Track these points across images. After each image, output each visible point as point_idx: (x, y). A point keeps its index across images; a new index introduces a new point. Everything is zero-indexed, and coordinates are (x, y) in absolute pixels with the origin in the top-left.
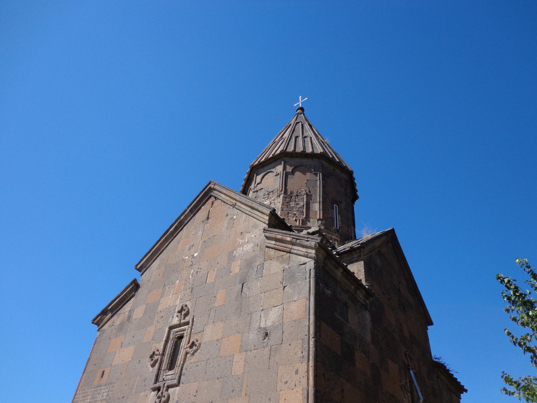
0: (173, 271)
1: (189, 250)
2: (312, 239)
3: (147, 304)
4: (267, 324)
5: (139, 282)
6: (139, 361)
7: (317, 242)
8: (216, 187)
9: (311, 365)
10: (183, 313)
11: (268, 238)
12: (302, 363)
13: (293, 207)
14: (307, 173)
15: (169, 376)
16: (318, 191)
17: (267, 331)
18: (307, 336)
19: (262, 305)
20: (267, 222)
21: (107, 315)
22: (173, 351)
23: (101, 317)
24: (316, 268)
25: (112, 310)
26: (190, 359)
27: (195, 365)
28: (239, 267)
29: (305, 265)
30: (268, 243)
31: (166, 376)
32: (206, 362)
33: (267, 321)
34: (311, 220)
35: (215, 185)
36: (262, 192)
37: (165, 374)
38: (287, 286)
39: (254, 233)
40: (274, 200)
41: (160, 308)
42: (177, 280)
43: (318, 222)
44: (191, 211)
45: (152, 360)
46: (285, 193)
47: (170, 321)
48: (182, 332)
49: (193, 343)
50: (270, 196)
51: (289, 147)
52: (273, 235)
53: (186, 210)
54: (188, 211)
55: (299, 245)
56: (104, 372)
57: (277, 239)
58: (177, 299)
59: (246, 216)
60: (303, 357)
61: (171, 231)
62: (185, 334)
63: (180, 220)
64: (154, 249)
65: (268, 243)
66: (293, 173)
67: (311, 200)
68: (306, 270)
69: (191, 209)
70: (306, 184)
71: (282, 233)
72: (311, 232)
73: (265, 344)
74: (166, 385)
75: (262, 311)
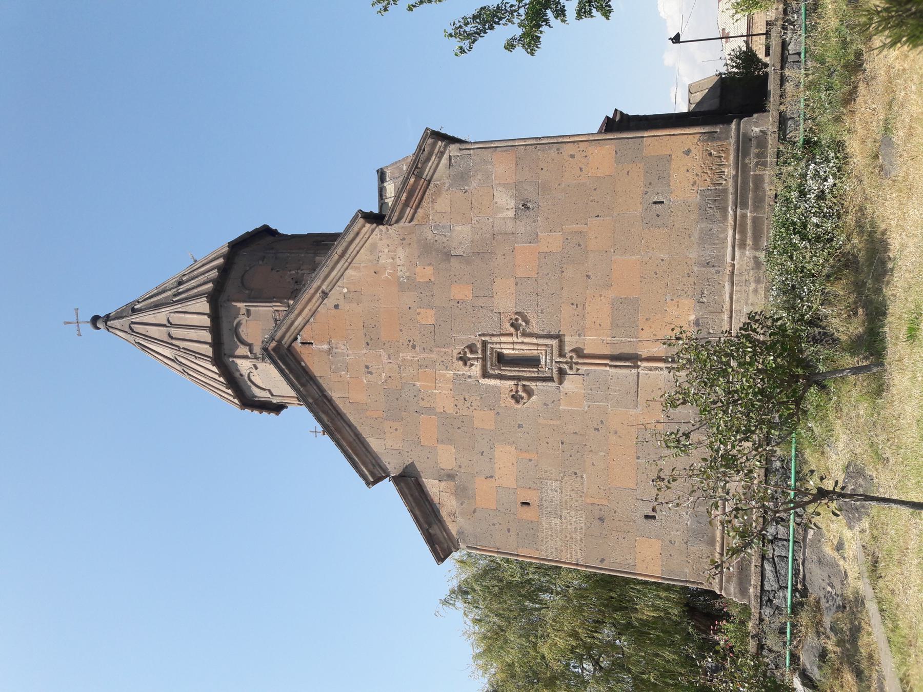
0: (397, 399)
6: (520, 426)
15: (548, 360)
20: (375, 225)
31: (546, 365)
37: (544, 366)
41: (450, 410)
45: (522, 398)
49: (512, 325)
55: (425, 165)
56: (523, 503)
58: (444, 376)
59: (351, 268)
70: (278, 271)
74: (558, 360)
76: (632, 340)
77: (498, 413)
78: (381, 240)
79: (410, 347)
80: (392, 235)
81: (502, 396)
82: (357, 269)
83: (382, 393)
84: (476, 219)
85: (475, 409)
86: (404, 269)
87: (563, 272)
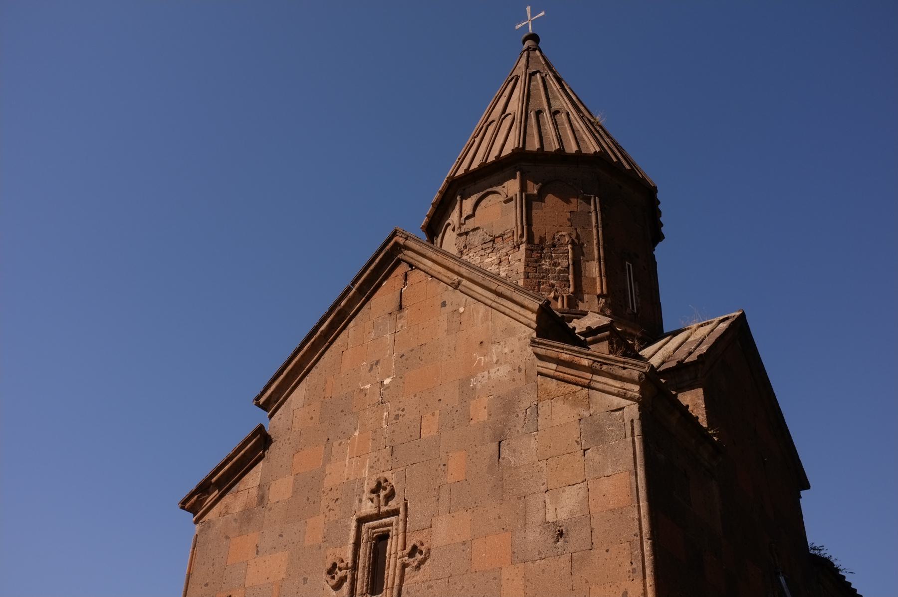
0: (342, 411)
1: (370, 371)
2: (633, 365)
3: (297, 474)
4: (559, 515)
5: (268, 430)
6: (305, 580)
7: (644, 371)
8: (410, 243)
9: (651, 583)
10: (383, 493)
11: (540, 357)
12: (633, 580)
13: (547, 271)
14: (572, 200)
16: (595, 237)
17: (561, 529)
18: (637, 536)
19: (545, 481)
20: (534, 325)
21: (210, 494)
22: (372, 562)
23: (198, 498)
24: (642, 418)
25: (219, 485)
26: (412, 575)
27: (426, 586)
28: (486, 410)
29: (621, 412)
30: (542, 367)
32: (447, 581)
33: (559, 510)
34: (586, 297)
35: (406, 239)
36: (478, 235)
38: (589, 449)
39: (508, 344)
40: (507, 255)
41: (328, 483)
42: (355, 430)
43: (599, 300)
44: (361, 291)
45: (333, 578)
46: (530, 240)
48: (385, 529)
49: (415, 548)
50: (497, 246)
51: (527, 139)
52: (552, 353)
53: (349, 289)
54: (354, 290)
55: (608, 375)
57: (561, 360)
58: (363, 466)
59: (487, 311)
60: (634, 570)
61: (322, 332)
62: (393, 532)
63: (338, 308)
64: (290, 367)
65: (542, 367)
66: (541, 197)
67: (583, 256)
68: (623, 421)
69: (361, 285)
70: (569, 220)
71: (571, 350)
72: (595, 327)
73: (560, 550)
75: (546, 492)
78: (519, 340)
79: (397, 412)
80: (525, 353)
81: (338, 550)
82: (486, 318)
83: (350, 390)
84: (544, 465)
85: (326, 517)
86: (485, 381)
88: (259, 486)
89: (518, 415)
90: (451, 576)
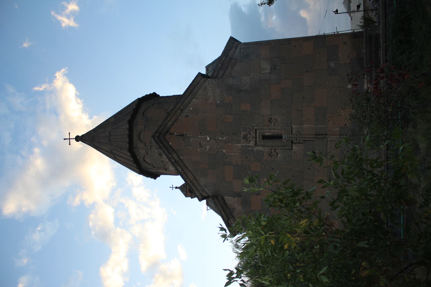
28: (229, 96)
47: (251, 148)
48: (261, 135)
68: (244, 48)
74: (291, 136)
76: (325, 126)
77: (262, 163)
87: (292, 96)
88: (234, 197)
89: (234, 84)
90: (281, 106)
